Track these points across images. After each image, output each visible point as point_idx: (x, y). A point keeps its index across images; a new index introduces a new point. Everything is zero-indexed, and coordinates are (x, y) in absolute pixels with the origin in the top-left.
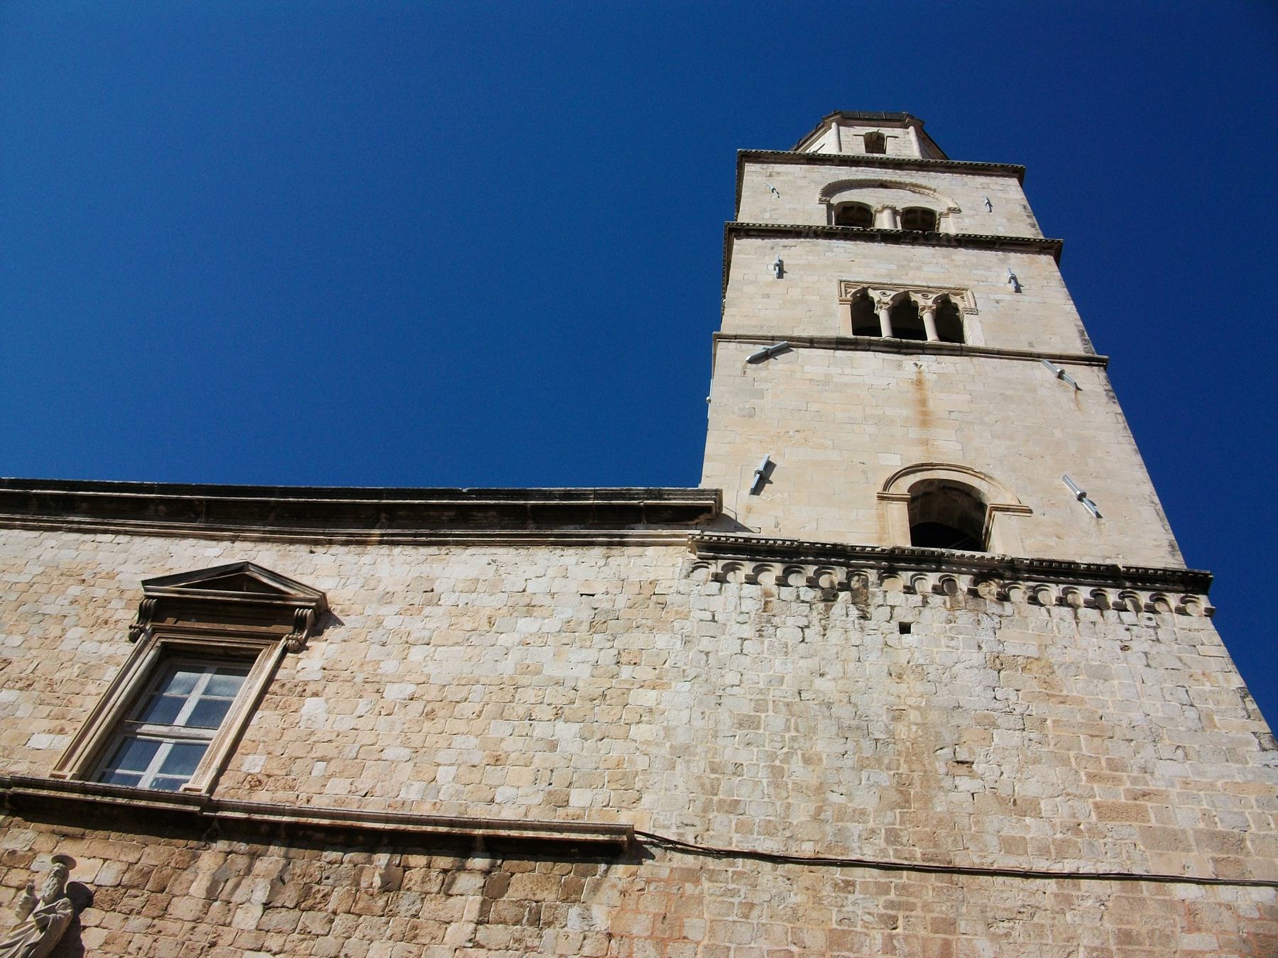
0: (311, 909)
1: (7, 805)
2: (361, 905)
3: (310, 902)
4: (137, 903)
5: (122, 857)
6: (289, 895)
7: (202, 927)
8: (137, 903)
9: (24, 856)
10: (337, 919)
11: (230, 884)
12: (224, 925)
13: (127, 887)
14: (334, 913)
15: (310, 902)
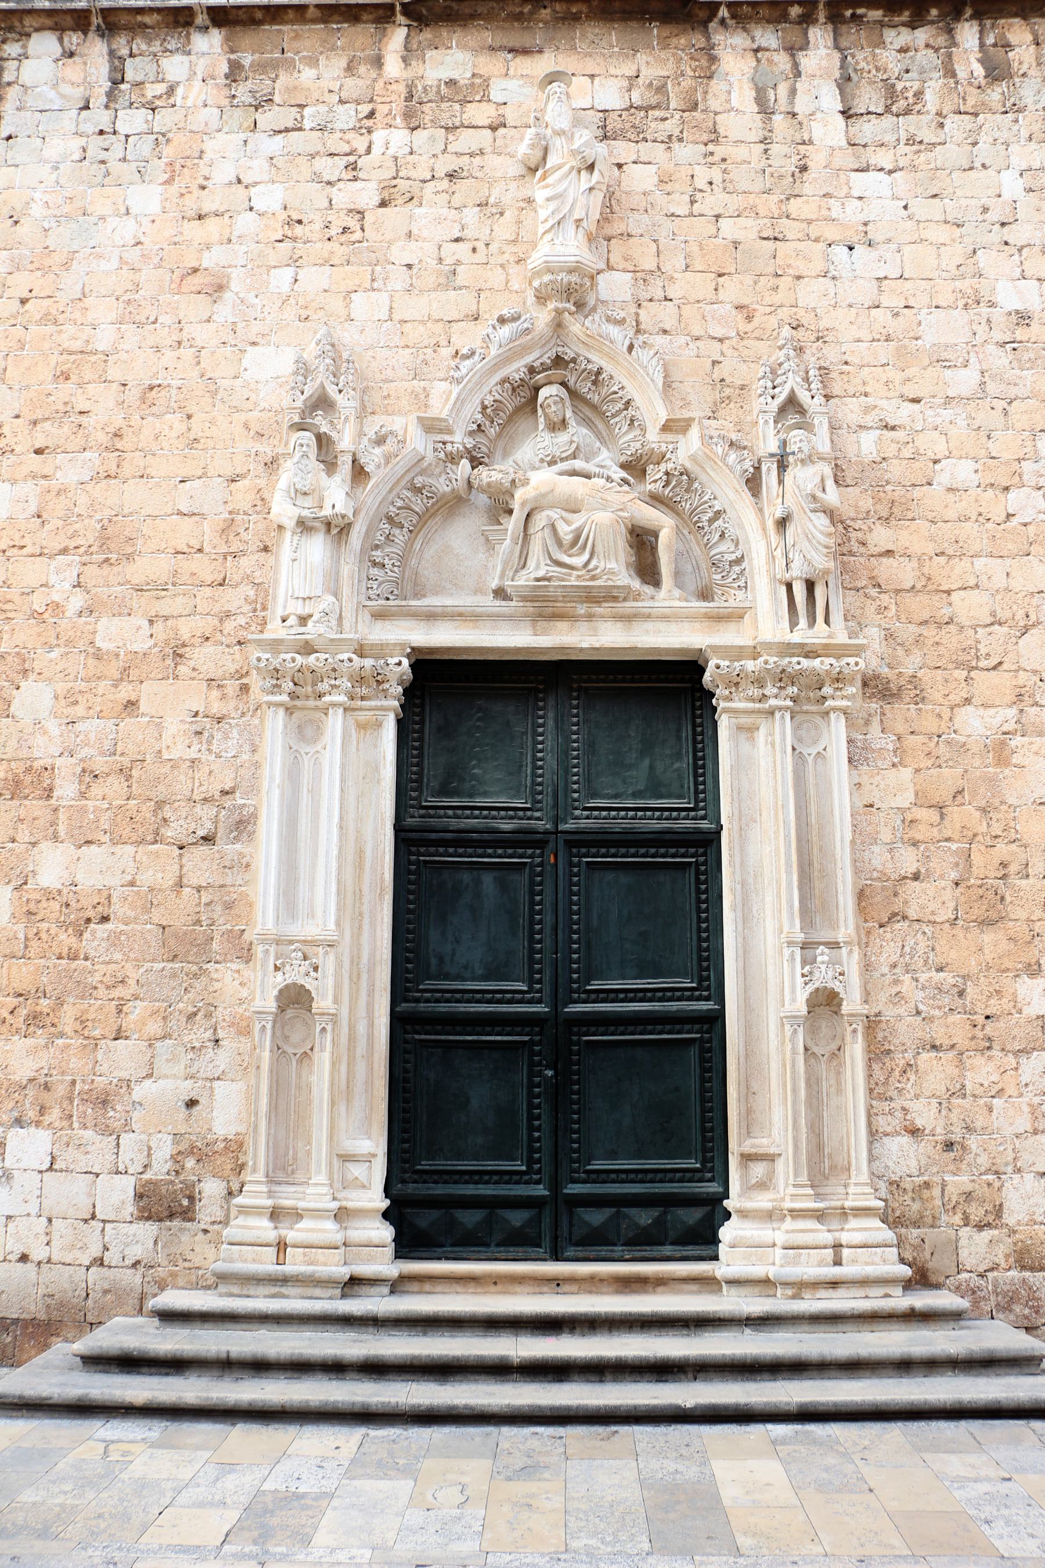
0: (907, 112)
1: (400, 18)
2: (971, 101)
3: (902, 104)
4: (671, 126)
5: (612, 71)
6: (868, 98)
7: (775, 149)
8: (671, 126)
9: (472, 85)
10: (948, 122)
11: (783, 89)
12: (804, 143)
13: (647, 109)
14: (939, 114)
15: (902, 104)
